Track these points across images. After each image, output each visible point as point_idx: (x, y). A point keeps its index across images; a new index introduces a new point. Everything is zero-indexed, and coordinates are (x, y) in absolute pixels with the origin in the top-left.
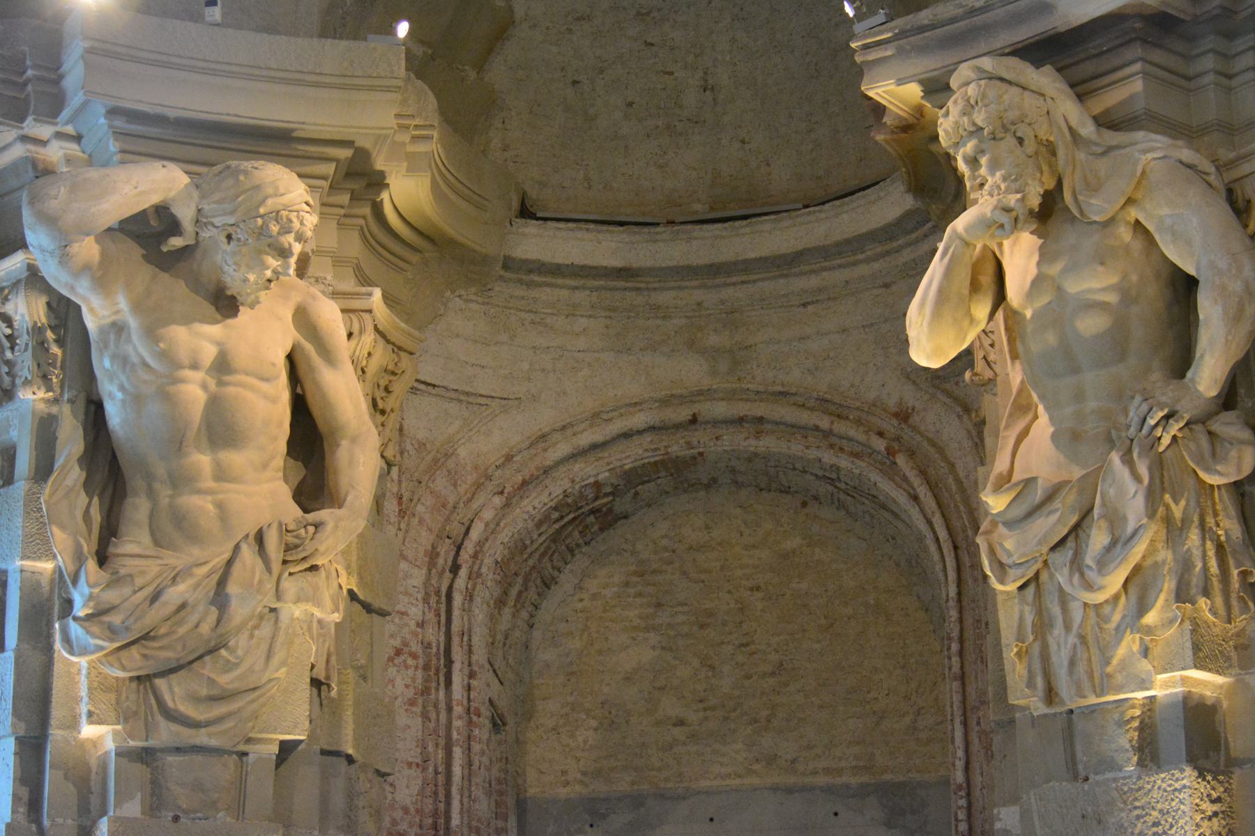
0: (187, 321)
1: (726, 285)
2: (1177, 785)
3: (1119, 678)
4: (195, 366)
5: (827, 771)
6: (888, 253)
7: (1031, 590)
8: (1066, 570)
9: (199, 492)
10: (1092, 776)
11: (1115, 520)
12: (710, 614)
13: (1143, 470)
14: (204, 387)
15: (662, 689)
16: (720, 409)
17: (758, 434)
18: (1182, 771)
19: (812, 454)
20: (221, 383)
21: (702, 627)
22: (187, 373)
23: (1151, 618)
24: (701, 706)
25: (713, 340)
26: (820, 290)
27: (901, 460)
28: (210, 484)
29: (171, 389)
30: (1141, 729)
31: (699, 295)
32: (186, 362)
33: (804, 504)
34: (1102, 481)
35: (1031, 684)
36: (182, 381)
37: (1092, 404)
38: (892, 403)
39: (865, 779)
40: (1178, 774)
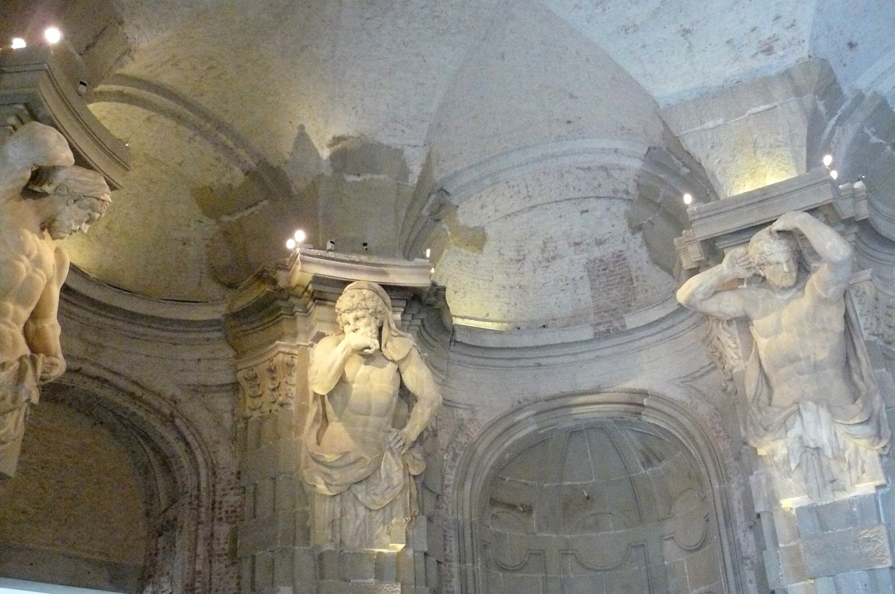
0: (33, 232)
1: (105, 316)
2: (394, 590)
3: (375, 542)
4: (28, 256)
5: (89, 551)
6: (183, 331)
7: (338, 499)
8: (364, 493)
9: (5, 323)
10: (352, 581)
11: (388, 477)
12: (47, 462)
13: (400, 461)
14: (27, 269)
15: (20, 493)
16: (93, 371)
17: (102, 387)
18: (398, 584)
19: (126, 405)
20: (34, 270)
21: (43, 468)
22: (24, 258)
23: (393, 521)
24: (37, 506)
25: (90, 337)
26: (143, 335)
27: (177, 421)
28: (9, 321)
29: (17, 262)
30: (376, 564)
31: (90, 315)
32: (27, 252)
33: (95, 424)
34: (385, 462)
35: (334, 535)
36: (21, 261)
37: (369, 430)
38: (169, 394)
39: (105, 559)
40: (394, 585)
